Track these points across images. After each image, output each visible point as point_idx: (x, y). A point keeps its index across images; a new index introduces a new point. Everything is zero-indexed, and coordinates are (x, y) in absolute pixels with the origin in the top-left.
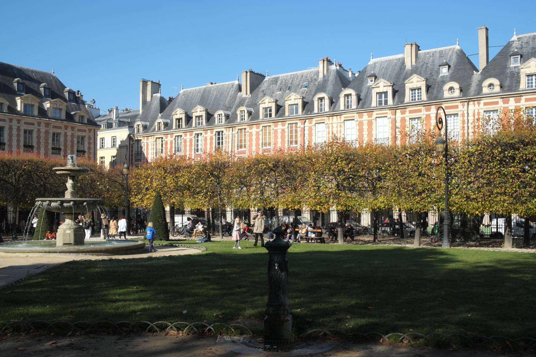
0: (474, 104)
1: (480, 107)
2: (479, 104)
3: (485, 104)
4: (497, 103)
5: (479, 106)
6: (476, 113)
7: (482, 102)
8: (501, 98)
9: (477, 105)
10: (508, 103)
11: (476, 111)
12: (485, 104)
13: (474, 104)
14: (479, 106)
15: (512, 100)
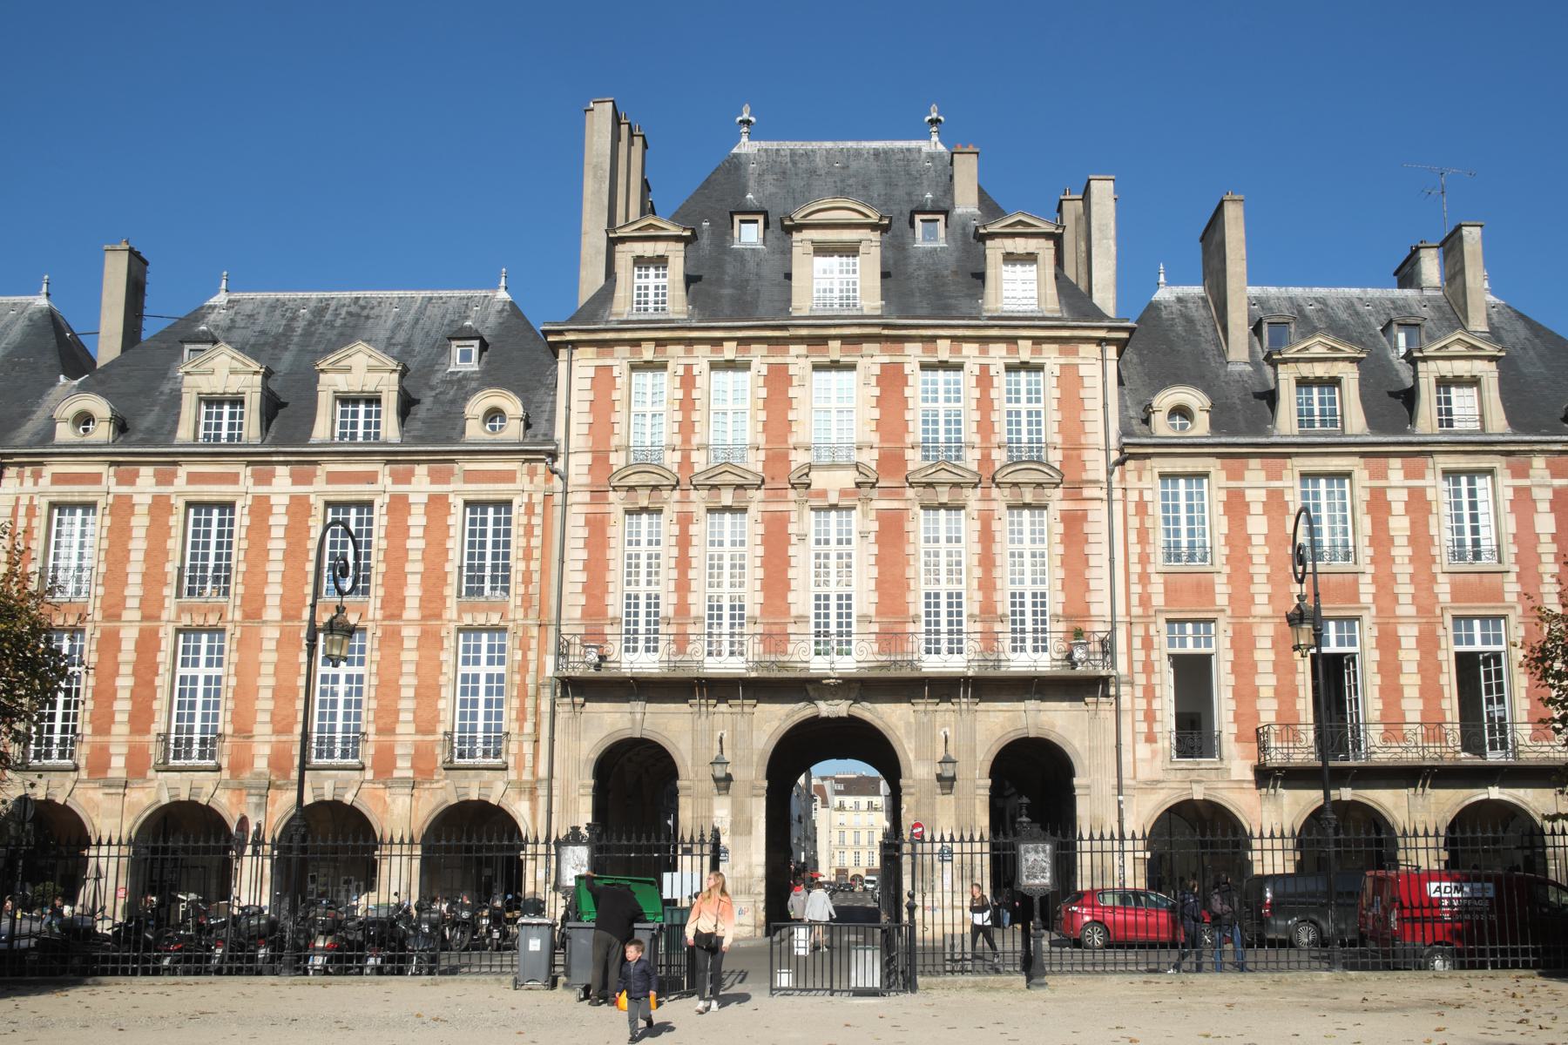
0: (20, 476)
1: (37, 489)
2: (37, 476)
3: (58, 479)
4: (96, 479)
5: (36, 483)
6: (22, 511)
7: (48, 471)
8: (112, 464)
9: (29, 482)
10: (133, 483)
11: (25, 501)
12: (58, 479)
13: (20, 476)
14: (36, 483)
15: (146, 473)
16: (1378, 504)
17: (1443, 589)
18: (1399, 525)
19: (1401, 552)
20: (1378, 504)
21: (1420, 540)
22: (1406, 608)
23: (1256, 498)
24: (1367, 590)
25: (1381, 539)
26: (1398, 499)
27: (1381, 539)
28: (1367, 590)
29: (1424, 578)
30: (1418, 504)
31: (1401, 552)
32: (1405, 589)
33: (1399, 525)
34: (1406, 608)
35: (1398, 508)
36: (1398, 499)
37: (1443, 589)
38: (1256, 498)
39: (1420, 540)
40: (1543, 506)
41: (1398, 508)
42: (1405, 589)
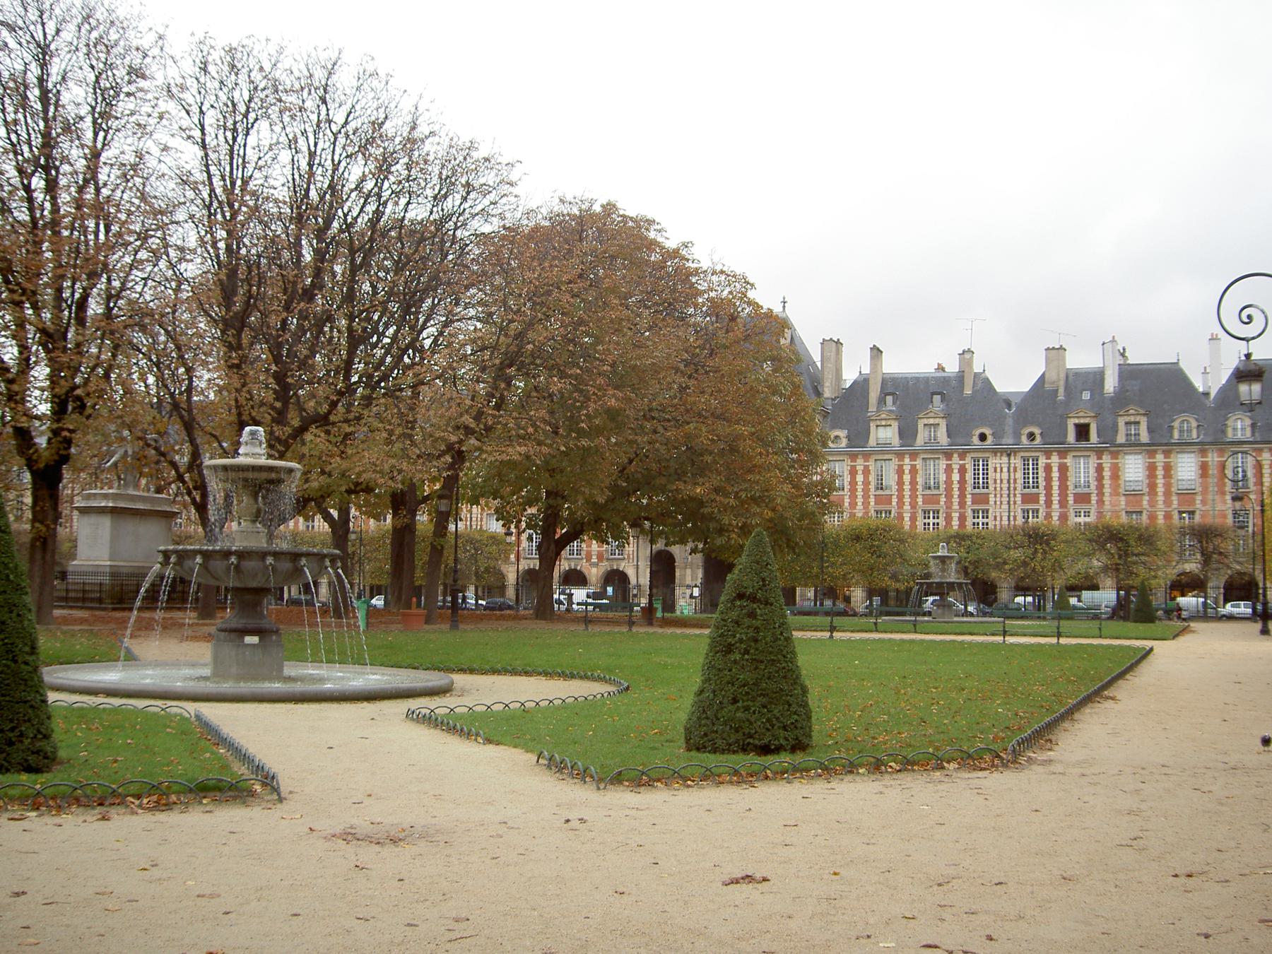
16: (900, 472)
17: (920, 500)
18: (907, 478)
19: (907, 487)
20: (900, 472)
21: (913, 483)
22: (907, 507)
23: (860, 468)
24: (895, 500)
25: (900, 483)
26: (907, 469)
27: (900, 483)
28: (895, 500)
29: (913, 497)
30: (914, 471)
31: (907, 487)
32: (907, 500)
33: (907, 478)
34: (907, 507)
35: (907, 471)
36: (907, 469)
37: (920, 500)
38: (860, 468)
39: (913, 483)
40: (956, 471)
41: (907, 471)
42: (907, 500)
